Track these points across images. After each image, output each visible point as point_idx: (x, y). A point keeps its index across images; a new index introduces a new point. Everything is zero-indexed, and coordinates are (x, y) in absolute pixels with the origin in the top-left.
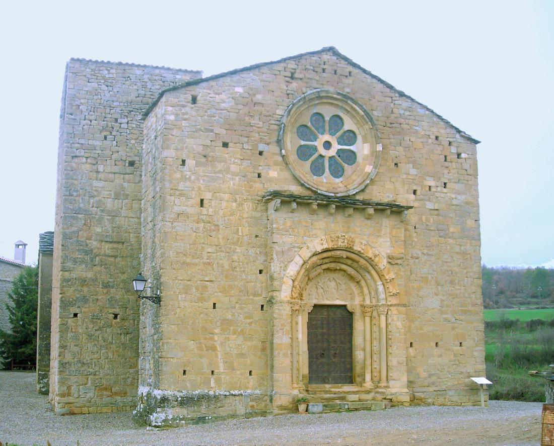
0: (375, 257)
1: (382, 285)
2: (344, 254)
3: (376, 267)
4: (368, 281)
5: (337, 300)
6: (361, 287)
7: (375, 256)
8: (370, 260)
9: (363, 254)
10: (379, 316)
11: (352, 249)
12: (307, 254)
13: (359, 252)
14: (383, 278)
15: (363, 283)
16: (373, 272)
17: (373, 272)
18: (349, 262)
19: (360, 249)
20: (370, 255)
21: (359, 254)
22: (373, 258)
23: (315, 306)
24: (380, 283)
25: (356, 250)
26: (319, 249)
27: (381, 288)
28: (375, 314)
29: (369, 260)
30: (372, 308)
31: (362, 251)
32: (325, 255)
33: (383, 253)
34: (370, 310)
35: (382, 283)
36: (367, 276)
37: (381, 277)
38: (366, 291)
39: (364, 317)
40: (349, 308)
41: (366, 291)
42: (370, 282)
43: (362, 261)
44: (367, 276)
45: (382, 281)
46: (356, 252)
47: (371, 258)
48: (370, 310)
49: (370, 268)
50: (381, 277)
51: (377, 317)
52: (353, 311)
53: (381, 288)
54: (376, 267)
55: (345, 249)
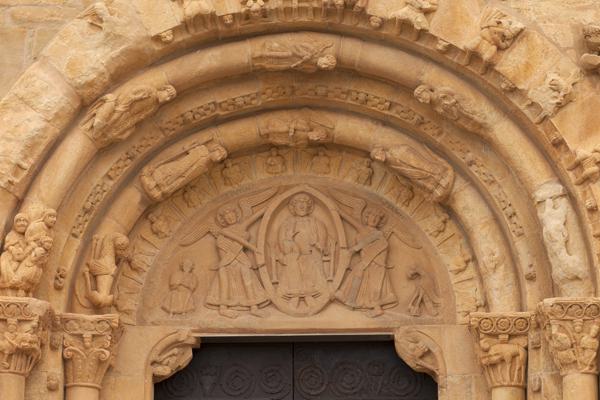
0: (499, 49)
1: (563, 203)
2: (325, 51)
3: (515, 101)
4: (493, 191)
5: (335, 309)
6: (466, 235)
7: (505, 42)
8: (476, 70)
9: (434, 38)
10: (559, 379)
11: (363, 15)
12: (94, 58)
13: (405, 25)
14: (564, 163)
15: (468, 204)
16: (505, 133)
17: (505, 133)
18: (378, 97)
19: (403, 12)
20: (467, 40)
21: (405, 36)
22: (488, 52)
23: (208, 348)
24: (546, 189)
25: (384, 22)
26: (165, 20)
27: (555, 218)
28: (539, 371)
29: (473, 68)
30: (522, 341)
31: (419, 21)
32: (209, 60)
33: (550, 29)
34: (507, 350)
35: (559, 189)
36: (484, 169)
37: (550, 150)
38: (487, 244)
39: (489, 392)
40: (406, 350)
41: (487, 244)
42: (503, 192)
43: (439, 84)
44: (484, 169)
45: (561, 181)
46: (391, 32)
47: (474, 56)
48: (507, 350)
49: (481, 109)
50: (550, 150)
51: (549, 385)
52: (427, 364)
53: (555, 218)
54: (515, 101)
55: (319, 20)
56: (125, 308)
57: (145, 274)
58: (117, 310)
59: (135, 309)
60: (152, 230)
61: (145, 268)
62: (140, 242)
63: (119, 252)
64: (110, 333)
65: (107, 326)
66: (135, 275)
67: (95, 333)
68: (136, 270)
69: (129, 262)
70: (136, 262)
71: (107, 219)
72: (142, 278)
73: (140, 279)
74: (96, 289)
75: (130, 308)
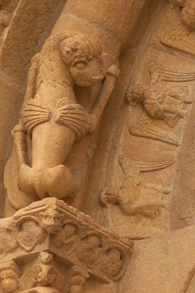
56: (140, 203)
57: (182, 123)
58: (124, 212)
59: (167, 201)
60: (183, 23)
61: (179, 108)
62: (162, 56)
63: (75, 71)
64: (45, 246)
65: (36, 230)
66: (160, 130)
67: (20, 253)
68: (158, 117)
69: (140, 101)
70: (155, 97)
71: (63, 16)
72: (175, 134)
73: (172, 136)
74: (29, 162)
75: (153, 201)
